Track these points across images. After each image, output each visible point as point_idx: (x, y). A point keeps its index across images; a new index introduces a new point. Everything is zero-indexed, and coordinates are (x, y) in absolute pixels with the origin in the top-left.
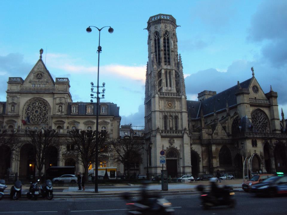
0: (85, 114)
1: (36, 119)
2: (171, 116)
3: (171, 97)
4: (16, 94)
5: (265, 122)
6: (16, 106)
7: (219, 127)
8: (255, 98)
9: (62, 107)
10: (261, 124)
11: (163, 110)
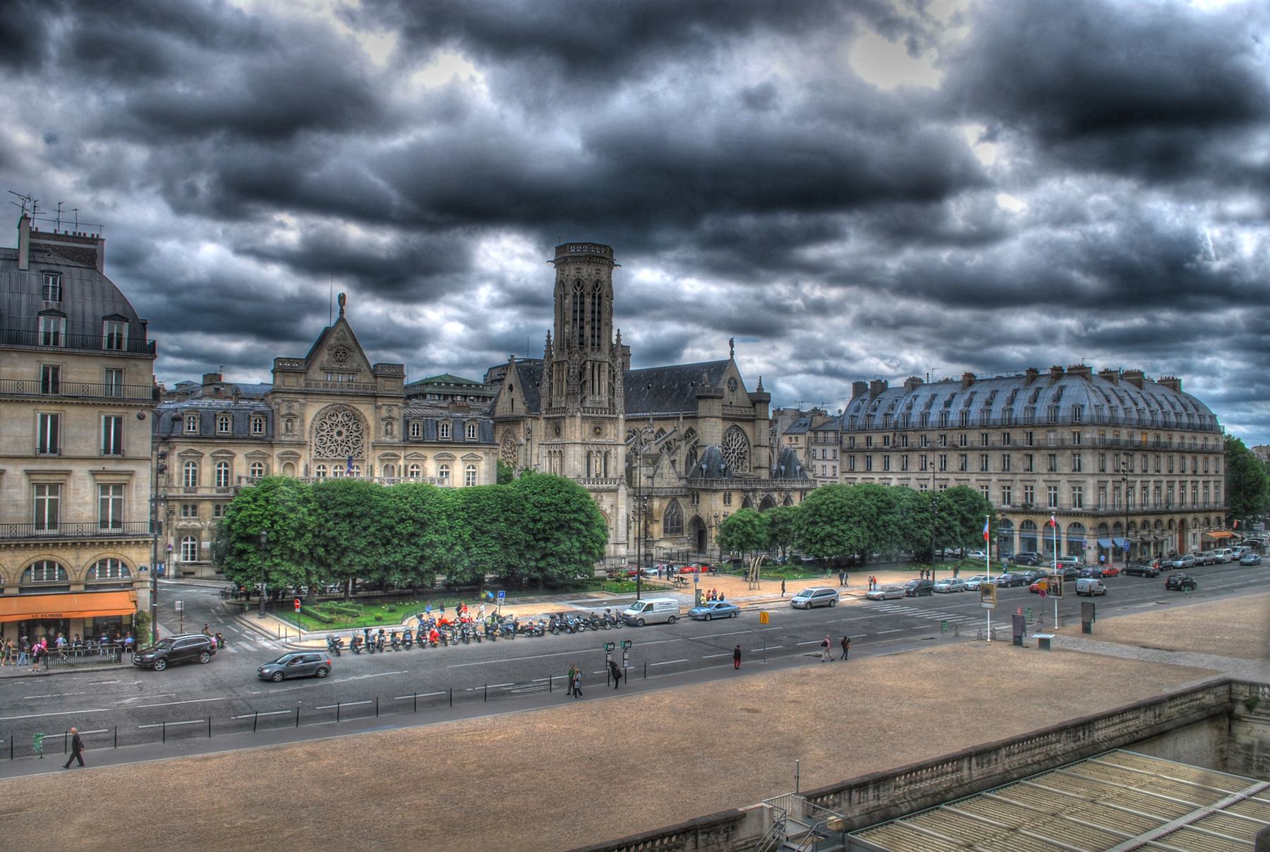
0: (437, 439)
1: (339, 449)
2: (599, 452)
3: (601, 415)
4: (297, 396)
5: (743, 451)
6: (297, 423)
7: (665, 461)
9: (391, 424)
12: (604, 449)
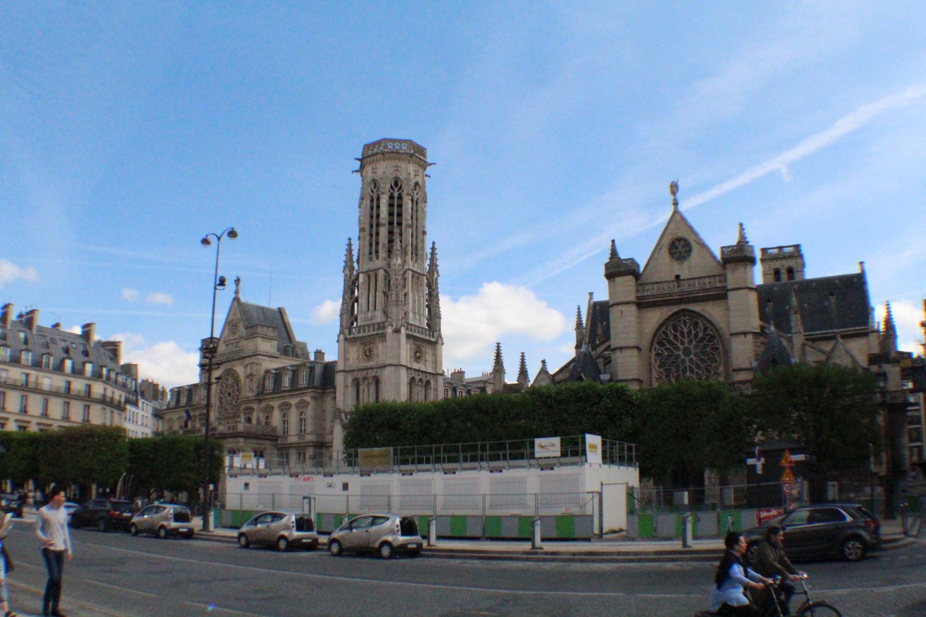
8: (678, 277)
10: (692, 356)
11: (355, 367)
12: (371, 374)
